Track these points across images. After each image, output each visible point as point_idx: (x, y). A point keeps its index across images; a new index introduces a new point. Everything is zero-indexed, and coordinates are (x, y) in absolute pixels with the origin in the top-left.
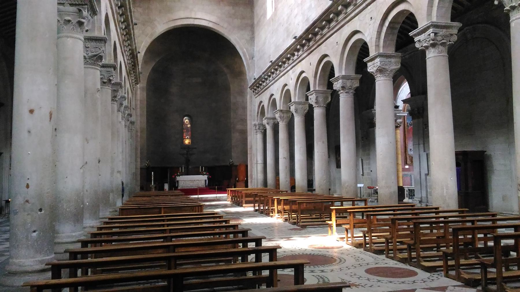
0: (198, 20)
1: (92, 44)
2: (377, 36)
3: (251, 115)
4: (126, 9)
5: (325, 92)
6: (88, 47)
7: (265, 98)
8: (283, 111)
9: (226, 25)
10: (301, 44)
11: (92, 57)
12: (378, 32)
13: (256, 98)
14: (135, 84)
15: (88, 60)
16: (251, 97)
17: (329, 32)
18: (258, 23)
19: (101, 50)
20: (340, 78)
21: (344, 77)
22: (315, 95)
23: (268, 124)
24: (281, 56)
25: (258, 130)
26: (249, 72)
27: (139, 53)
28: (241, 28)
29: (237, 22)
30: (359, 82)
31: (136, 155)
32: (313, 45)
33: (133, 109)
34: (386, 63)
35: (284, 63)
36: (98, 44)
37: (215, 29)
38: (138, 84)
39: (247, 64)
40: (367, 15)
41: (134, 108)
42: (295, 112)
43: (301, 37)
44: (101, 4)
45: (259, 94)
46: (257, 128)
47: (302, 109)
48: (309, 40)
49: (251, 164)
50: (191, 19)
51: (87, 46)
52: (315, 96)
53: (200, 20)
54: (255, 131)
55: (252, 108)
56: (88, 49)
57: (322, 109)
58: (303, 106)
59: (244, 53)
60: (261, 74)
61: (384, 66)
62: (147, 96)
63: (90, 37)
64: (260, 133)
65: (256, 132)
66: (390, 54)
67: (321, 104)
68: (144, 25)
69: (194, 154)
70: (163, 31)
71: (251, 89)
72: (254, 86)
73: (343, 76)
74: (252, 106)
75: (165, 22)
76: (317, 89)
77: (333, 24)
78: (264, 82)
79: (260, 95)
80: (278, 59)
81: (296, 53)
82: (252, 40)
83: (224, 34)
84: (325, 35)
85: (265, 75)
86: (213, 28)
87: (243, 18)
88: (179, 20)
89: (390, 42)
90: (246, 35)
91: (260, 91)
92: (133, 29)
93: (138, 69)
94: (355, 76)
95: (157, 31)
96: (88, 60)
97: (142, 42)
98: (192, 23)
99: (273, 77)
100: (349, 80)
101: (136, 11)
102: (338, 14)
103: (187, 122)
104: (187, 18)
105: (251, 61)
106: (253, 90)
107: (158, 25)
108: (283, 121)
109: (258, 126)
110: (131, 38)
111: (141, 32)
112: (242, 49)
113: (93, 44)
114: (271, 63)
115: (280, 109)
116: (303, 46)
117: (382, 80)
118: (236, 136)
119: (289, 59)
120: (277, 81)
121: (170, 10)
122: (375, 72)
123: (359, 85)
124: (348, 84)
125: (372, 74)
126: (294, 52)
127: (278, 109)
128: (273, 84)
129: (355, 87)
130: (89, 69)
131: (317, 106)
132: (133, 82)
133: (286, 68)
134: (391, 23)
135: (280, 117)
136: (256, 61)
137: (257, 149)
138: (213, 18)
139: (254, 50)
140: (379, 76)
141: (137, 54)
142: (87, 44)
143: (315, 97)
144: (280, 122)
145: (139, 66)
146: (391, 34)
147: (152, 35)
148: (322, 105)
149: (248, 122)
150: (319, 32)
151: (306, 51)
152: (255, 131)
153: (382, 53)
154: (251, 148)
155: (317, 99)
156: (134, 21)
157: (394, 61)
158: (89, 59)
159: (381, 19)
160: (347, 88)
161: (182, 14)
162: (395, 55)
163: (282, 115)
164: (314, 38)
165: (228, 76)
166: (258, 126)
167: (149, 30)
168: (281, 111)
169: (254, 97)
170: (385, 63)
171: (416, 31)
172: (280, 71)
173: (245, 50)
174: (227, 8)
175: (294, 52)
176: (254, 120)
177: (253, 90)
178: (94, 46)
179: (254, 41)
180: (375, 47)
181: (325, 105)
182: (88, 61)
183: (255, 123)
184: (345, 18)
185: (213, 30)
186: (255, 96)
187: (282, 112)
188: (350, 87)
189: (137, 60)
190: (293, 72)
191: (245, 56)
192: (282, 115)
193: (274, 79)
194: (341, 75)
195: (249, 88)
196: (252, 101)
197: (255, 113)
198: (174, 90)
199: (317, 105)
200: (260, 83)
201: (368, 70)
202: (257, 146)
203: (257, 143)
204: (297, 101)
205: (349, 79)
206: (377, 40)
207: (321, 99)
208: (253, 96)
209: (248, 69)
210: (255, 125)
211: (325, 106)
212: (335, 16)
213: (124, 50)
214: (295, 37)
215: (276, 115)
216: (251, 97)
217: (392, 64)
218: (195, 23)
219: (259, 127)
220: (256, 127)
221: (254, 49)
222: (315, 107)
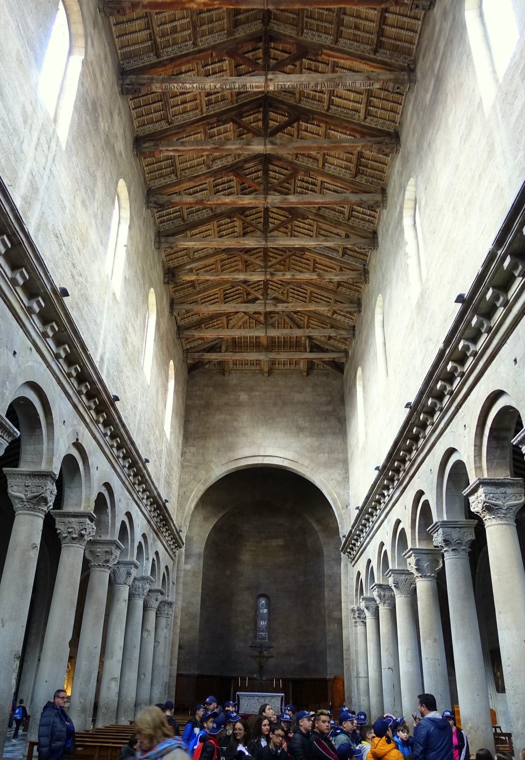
0: (269, 458)
1: (35, 481)
2: (475, 453)
3: (346, 594)
4: (122, 438)
5: (432, 552)
6: (28, 486)
7: (361, 566)
8: (383, 587)
9: (307, 463)
10: (387, 477)
11: (31, 499)
12: (475, 446)
13: (353, 566)
14: (176, 547)
15: (26, 503)
16: (346, 565)
17: (418, 455)
18: (351, 456)
19: (45, 489)
20: (438, 526)
21: (444, 524)
22: (415, 556)
23: (367, 608)
24: (368, 498)
25: (358, 620)
26: (342, 527)
27: (167, 501)
28: (328, 465)
29: (323, 457)
30: (473, 533)
31: (172, 654)
32: (404, 478)
33: (173, 583)
34: (497, 496)
35: (375, 508)
36: (42, 481)
37: (294, 470)
38: (180, 547)
39: (338, 516)
40: (460, 422)
41: (175, 583)
42: (395, 586)
43: (384, 466)
44: (54, 429)
45: (354, 560)
46: (357, 615)
47: (406, 582)
48: (397, 471)
49: (350, 677)
50: (259, 458)
51: (27, 484)
52: (414, 558)
53: (271, 458)
54: (354, 621)
55: (348, 582)
56: (27, 489)
57: (429, 580)
58: (407, 576)
59: (334, 500)
60: (350, 528)
61: (493, 502)
62: (204, 567)
63: (32, 472)
64: (361, 623)
65: (356, 622)
66: (502, 479)
67: (427, 571)
68: (196, 468)
69: (272, 657)
70: (221, 475)
71: (344, 553)
72: (346, 549)
73: (443, 522)
74: (348, 579)
75: (224, 463)
76: (417, 547)
77: (421, 442)
78: (357, 540)
79: (356, 562)
80: (365, 503)
81: (386, 493)
82: (345, 481)
83: (305, 475)
84: (415, 460)
85: (356, 530)
86: (289, 468)
87: (332, 452)
88: (244, 460)
89: (499, 461)
90: (336, 474)
91: (356, 556)
92: (145, 468)
93: (174, 525)
94: (465, 522)
95: (213, 475)
96: (26, 503)
97: (193, 490)
98: (260, 462)
99: (366, 533)
100: (455, 529)
101: (188, 451)
102: (423, 426)
103: (262, 605)
104: (254, 456)
105: (344, 511)
106: (346, 553)
107: (215, 467)
108: (384, 603)
109: (357, 612)
110: (147, 480)
111: (192, 477)
112: (331, 494)
113: (36, 481)
114: (357, 511)
115: (379, 583)
116: (392, 480)
117: (495, 525)
118: (331, 627)
119: (379, 502)
120: (372, 538)
121: (231, 447)
122: (480, 511)
123: (474, 538)
124: (455, 535)
125: (478, 516)
126: (384, 491)
127: (376, 582)
128: (368, 543)
129: (467, 540)
130: (26, 516)
131: (420, 576)
132: (170, 545)
133: (380, 516)
134: (491, 430)
135: (379, 596)
136: (351, 510)
137: (356, 652)
138: (290, 455)
139: (348, 495)
140: (489, 517)
141: (164, 504)
142: (27, 482)
143: (414, 560)
144: (380, 606)
145: (173, 521)
146: (498, 447)
147: (206, 480)
148: (429, 574)
149: (343, 605)
150: (406, 456)
151: (398, 488)
152: (354, 621)
153: (486, 479)
154: (348, 650)
155: (417, 563)
156: (144, 457)
157: (511, 492)
158: (28, 502)
159: (477, 426)
160: (453, 542)
161: (246, 452)
162: (511, 481)
163: (382, 593)
164: (402, 468)
165: (321, 535)
166: (357, 612)
167: (202, 474)
168: (380, 586)
169: (350, 565)
170: (495, 495)
171: (520, 435)
172: (373, 522)
173: (335, 495)
174: (309, 440)
175: (384, 491)
176: (352, 602)
177: (346, 553)
178: (36, 484)
179: (348, 482)
180: (476, 471)
181: (433, 575)
182: (25, 505)
183: (352, 606)
184: (434, 431)
185: (292, 471)
186: (351, 563)
187: (381, 588)
188: (458, 541)
189: (168, 512)
190: (388, 523)
191: (335, 503)
192: (382, 593)
193: (368, 535)
194: (439, 522)
195: (342, 551)
196: (347, 572)
197: (353, 590)
198: (246, 557)
199: (420, 575)
200: (353, 542)
201: (472, 510)
202: (356, 646)
203: (356, 641)
204: (397, 568)
205: (455, 528)
206: (477, 459)
207: (425, 564)
208: (349, 563)
209: (340, 523)
210: (353, 610)
211: (433, 576)
212: (420, 430)
213: (138, 497)
214: (377, 468)
215: (374, 592)
216: (346, 565)
217: (509, 498)
218: (265, 462)
219: (359, 614)
220: (354, 615)
221: (348, 493)
222: (417, 577)
